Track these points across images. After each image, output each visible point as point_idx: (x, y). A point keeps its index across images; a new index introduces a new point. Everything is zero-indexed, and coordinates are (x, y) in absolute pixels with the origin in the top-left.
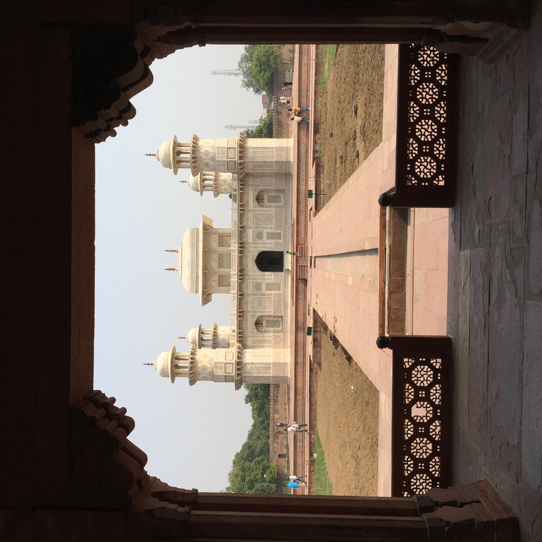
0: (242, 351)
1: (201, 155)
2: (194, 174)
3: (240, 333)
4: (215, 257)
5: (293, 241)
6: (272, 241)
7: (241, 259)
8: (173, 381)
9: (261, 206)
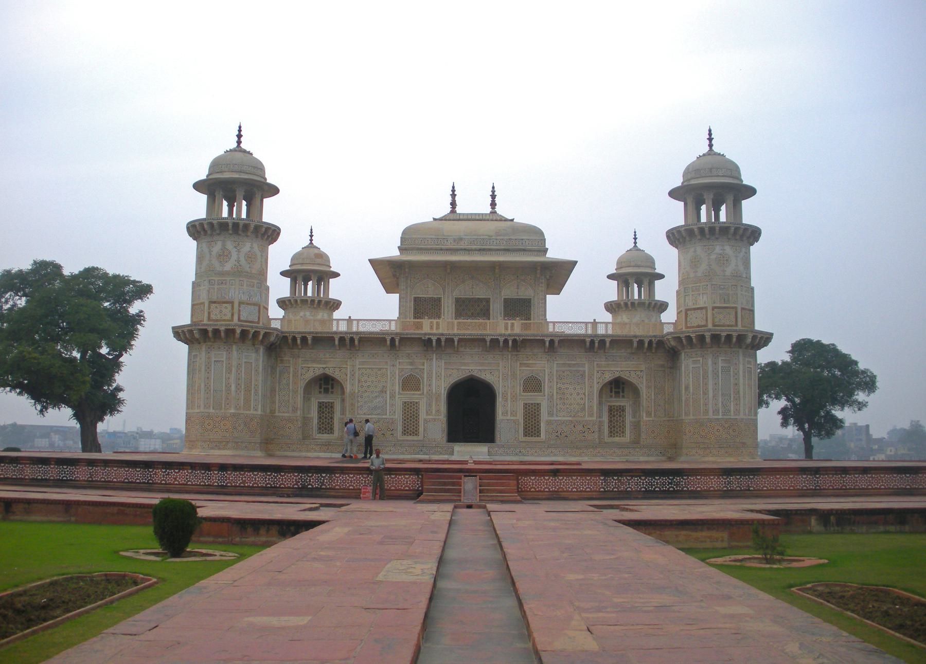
0: (262, 342)
1: (718, 250)
2: (675, 237)
3: (304, 339)
4: (480, 292)
5: (522, 463)
6: (520, 417)
7: (478, 342)
8: (198, 186)
9: (601, 391)
